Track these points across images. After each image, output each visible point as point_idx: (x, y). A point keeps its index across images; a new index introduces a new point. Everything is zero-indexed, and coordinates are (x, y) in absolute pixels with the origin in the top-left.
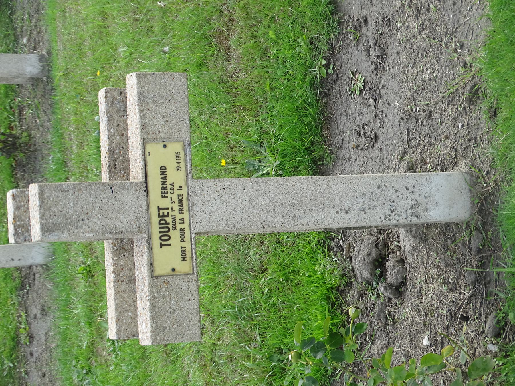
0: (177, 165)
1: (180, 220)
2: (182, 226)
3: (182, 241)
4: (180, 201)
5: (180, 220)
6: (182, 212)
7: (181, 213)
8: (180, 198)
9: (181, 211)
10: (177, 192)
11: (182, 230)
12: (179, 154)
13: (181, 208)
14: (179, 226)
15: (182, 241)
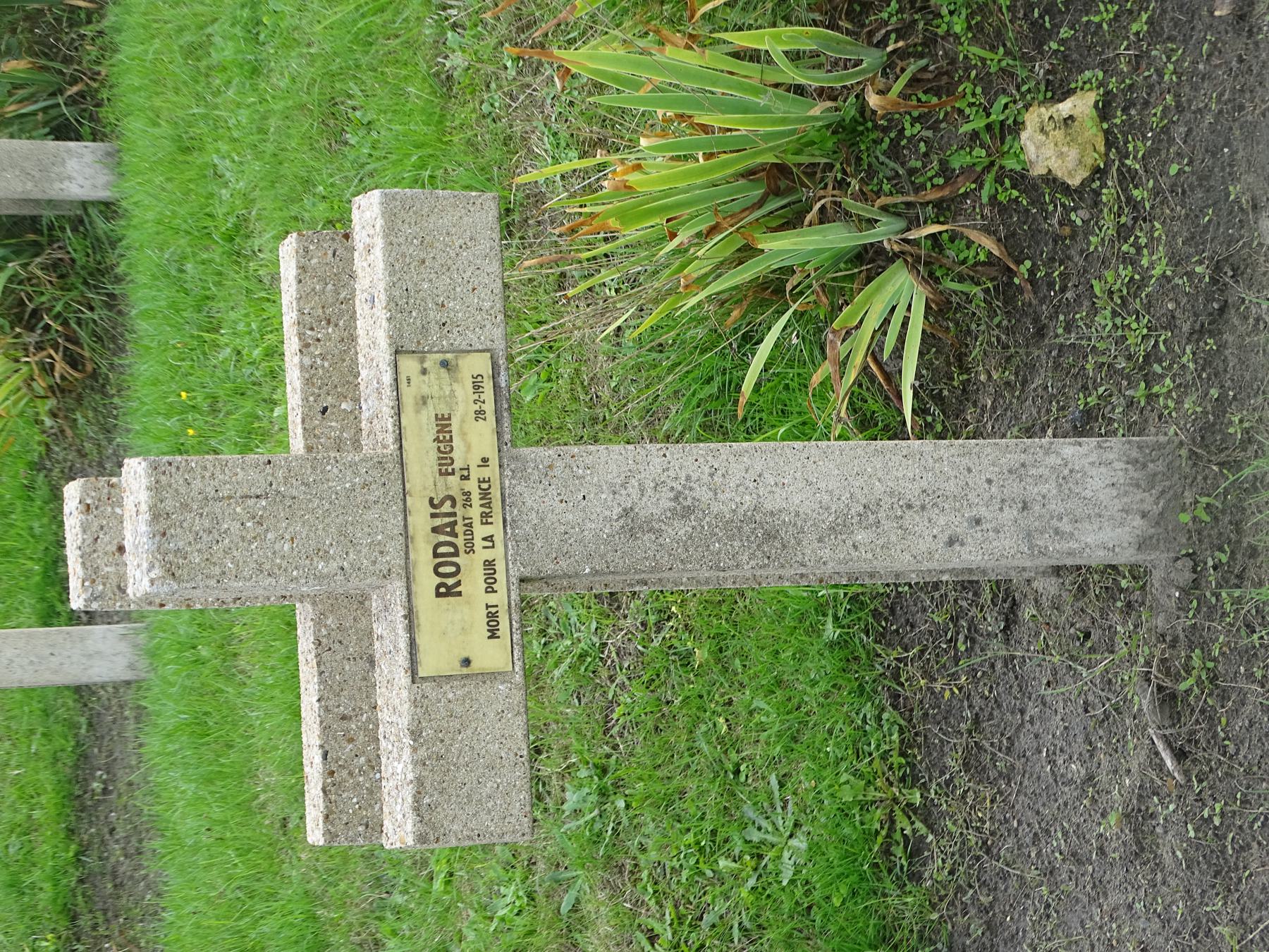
0: (477, 407)
1: (485, 539)
2: (489, 555)
3: (490, 590)
4: (485, 494)
5: (485, 539)
6: (490, 520)
7: (487, 523)
8: (485, 486)
9: (486, 518)
10: (476, 473)
11: (489, 564)
12: (480, 379)
13: (487, 510)
14: (482, 555)
15: (490, 590)
